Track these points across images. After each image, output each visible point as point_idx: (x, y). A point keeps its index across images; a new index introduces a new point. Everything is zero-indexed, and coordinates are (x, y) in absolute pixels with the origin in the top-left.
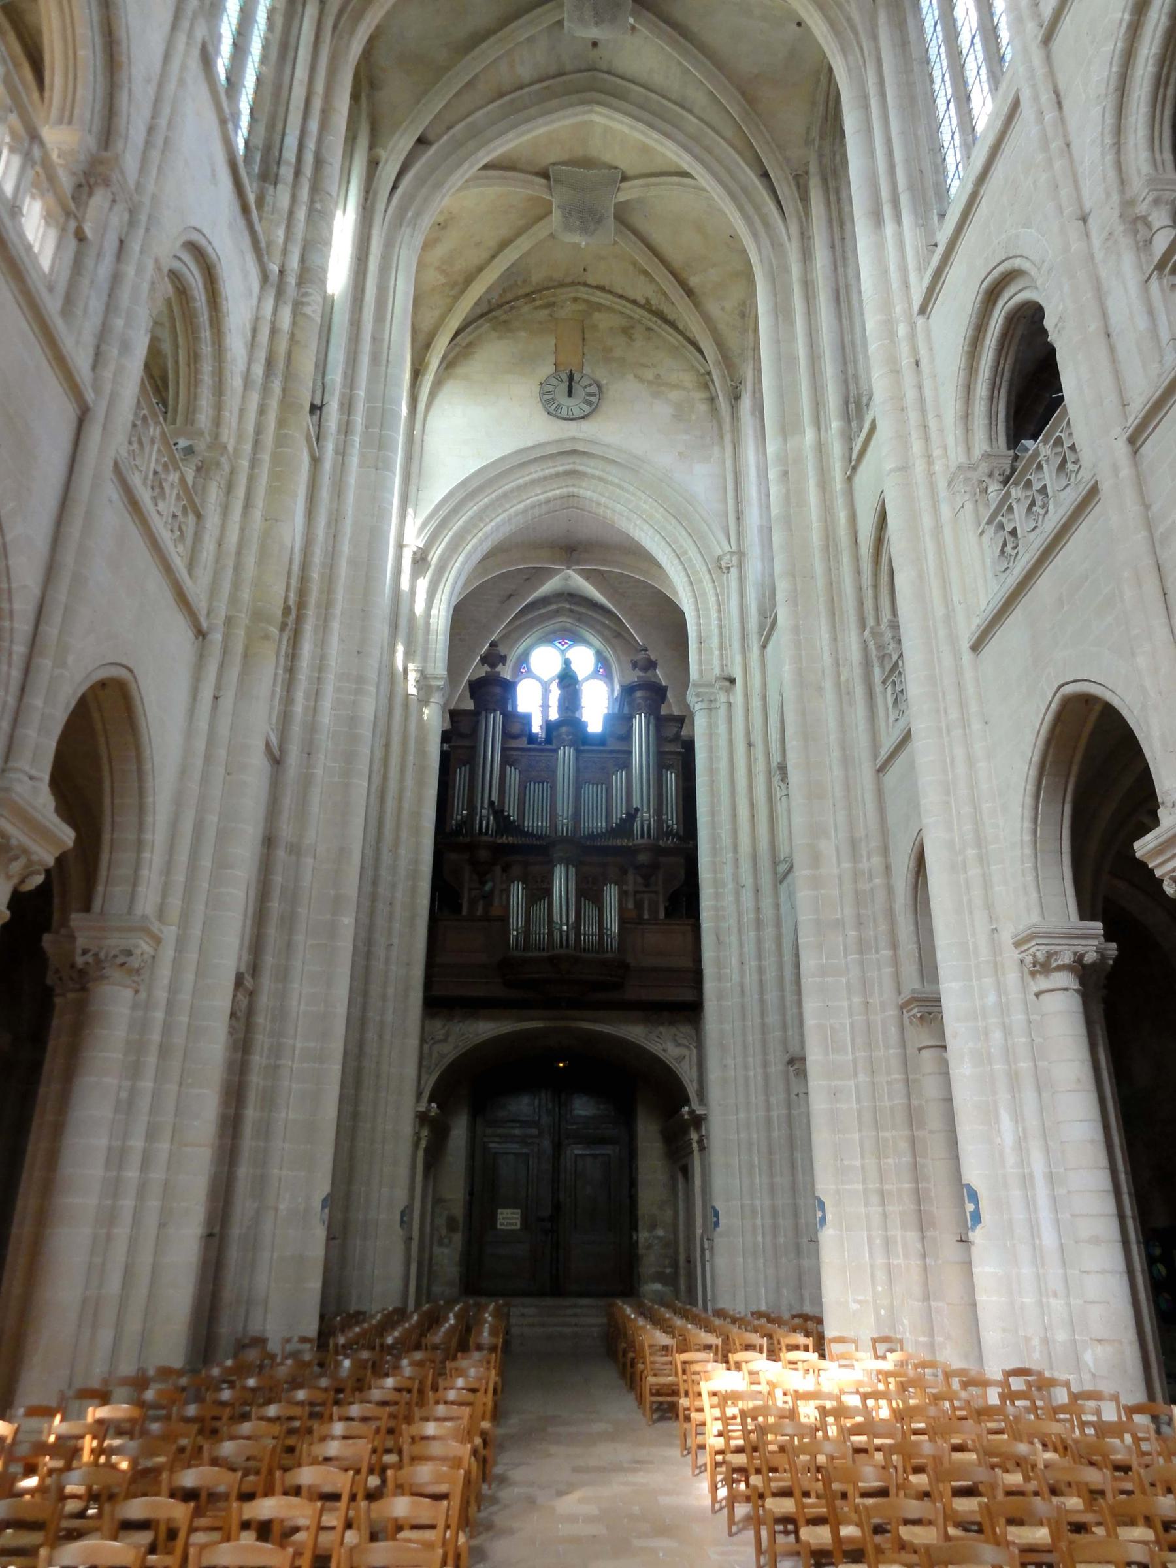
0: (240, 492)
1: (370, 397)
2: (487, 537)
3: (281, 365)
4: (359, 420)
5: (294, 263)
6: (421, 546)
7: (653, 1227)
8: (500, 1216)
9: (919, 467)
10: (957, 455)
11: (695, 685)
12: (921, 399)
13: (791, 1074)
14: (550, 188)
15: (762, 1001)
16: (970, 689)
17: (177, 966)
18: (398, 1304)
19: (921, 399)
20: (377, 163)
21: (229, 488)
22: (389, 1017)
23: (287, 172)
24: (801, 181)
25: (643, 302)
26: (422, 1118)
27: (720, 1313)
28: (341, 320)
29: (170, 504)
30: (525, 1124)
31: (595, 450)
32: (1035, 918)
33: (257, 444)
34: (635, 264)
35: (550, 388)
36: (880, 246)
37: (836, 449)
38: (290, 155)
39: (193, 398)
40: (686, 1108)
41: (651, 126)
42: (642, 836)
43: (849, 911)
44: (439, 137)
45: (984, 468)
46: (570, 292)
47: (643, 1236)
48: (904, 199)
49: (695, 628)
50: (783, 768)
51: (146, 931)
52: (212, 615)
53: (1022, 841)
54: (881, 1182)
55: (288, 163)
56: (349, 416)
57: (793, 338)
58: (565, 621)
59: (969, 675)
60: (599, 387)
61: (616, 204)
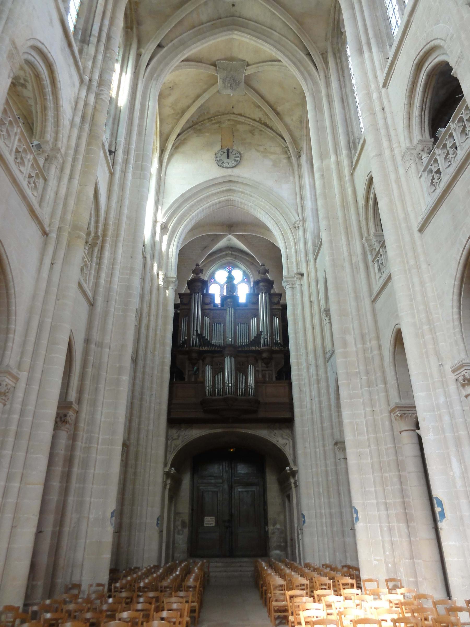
0: (67, 171)
1: (137, 149)
2: (193, 218)
3: (89, 118)
4: (132, 158)
5: (96, 76)
6: (165, 221)
7: (275, 524)
8: (205, 520)
9: (387, 153)
10: (405, 143)
11: (285, 277)
12: (386, 124)
13: (336, 450)
14: (217, 70)
15: (321, 416)
16: (420, 250)
17: (27, 392)
18: (156, 564)
19: (386, 124)
20: (141, 55)
21: (62, 170)
22: (151, 428)
23: (94, 40)
24: (324, 56)
25: (258, 119)
26: (167, 474)
27: (307, 566)
28: (124, 117)
29: (27, 169)
30: (216, 478)
31: (240, 180)
32: (463, 356)
33: (76, 152)
34: (254, 103)
35: (219, 155)
36: (362, 63)
37: (345, 162)
39: (44, 127)
40: (288, 468)
41: (258, 38)
42: (265, 345)
43: (362, 368)
44: (168, 44)
45: (420, 147)
46: (228, 117)
47: (270, 528)
48: (373, 41)
49: (285, 253)
50: (327, 312)
51: (10, 374)
52: (51, 225)
53: (453, 319)
54: (385, 499)
55: (94, 36)
56: (127, 156)
57: (323, 119)
58: (230, 259)
59: (418, 242)
60: (240, 154)
61: (245, 76)
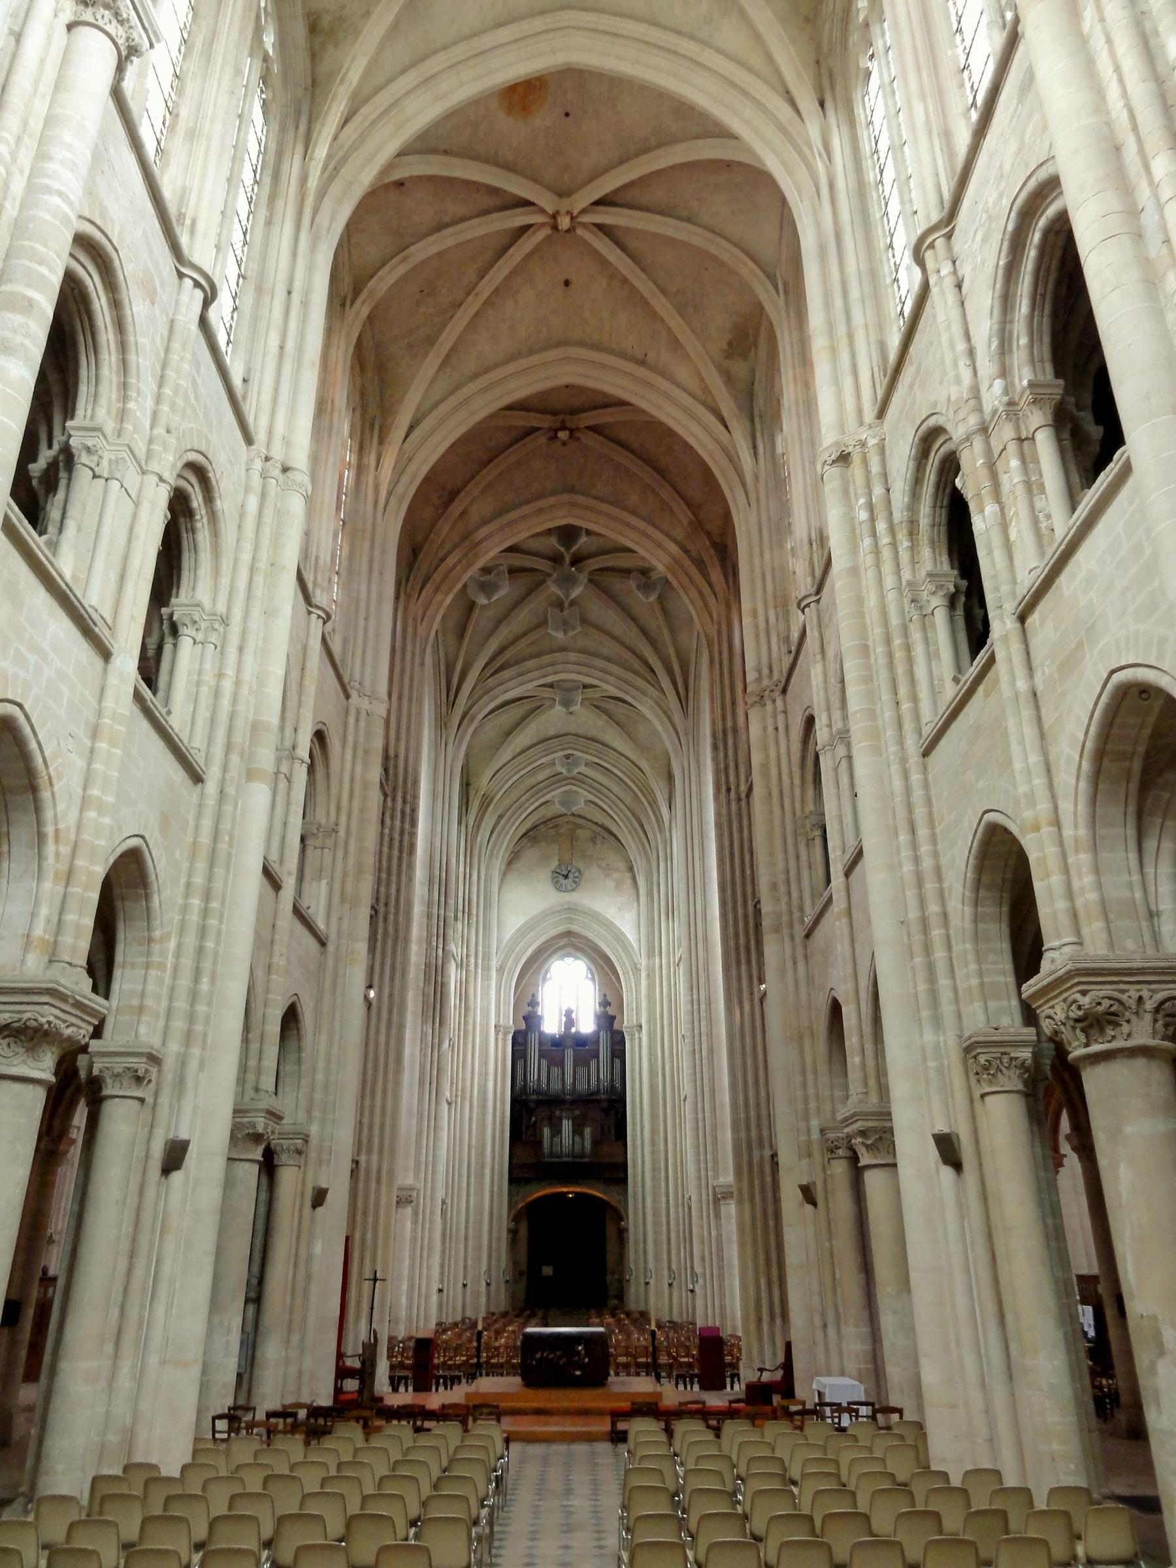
4: (480, 961)
7: (613, 1274)
23: (460, 915)
26: (509, 1231)
38: (460, 907)
46: (565, 819)
47: (609, 1278)
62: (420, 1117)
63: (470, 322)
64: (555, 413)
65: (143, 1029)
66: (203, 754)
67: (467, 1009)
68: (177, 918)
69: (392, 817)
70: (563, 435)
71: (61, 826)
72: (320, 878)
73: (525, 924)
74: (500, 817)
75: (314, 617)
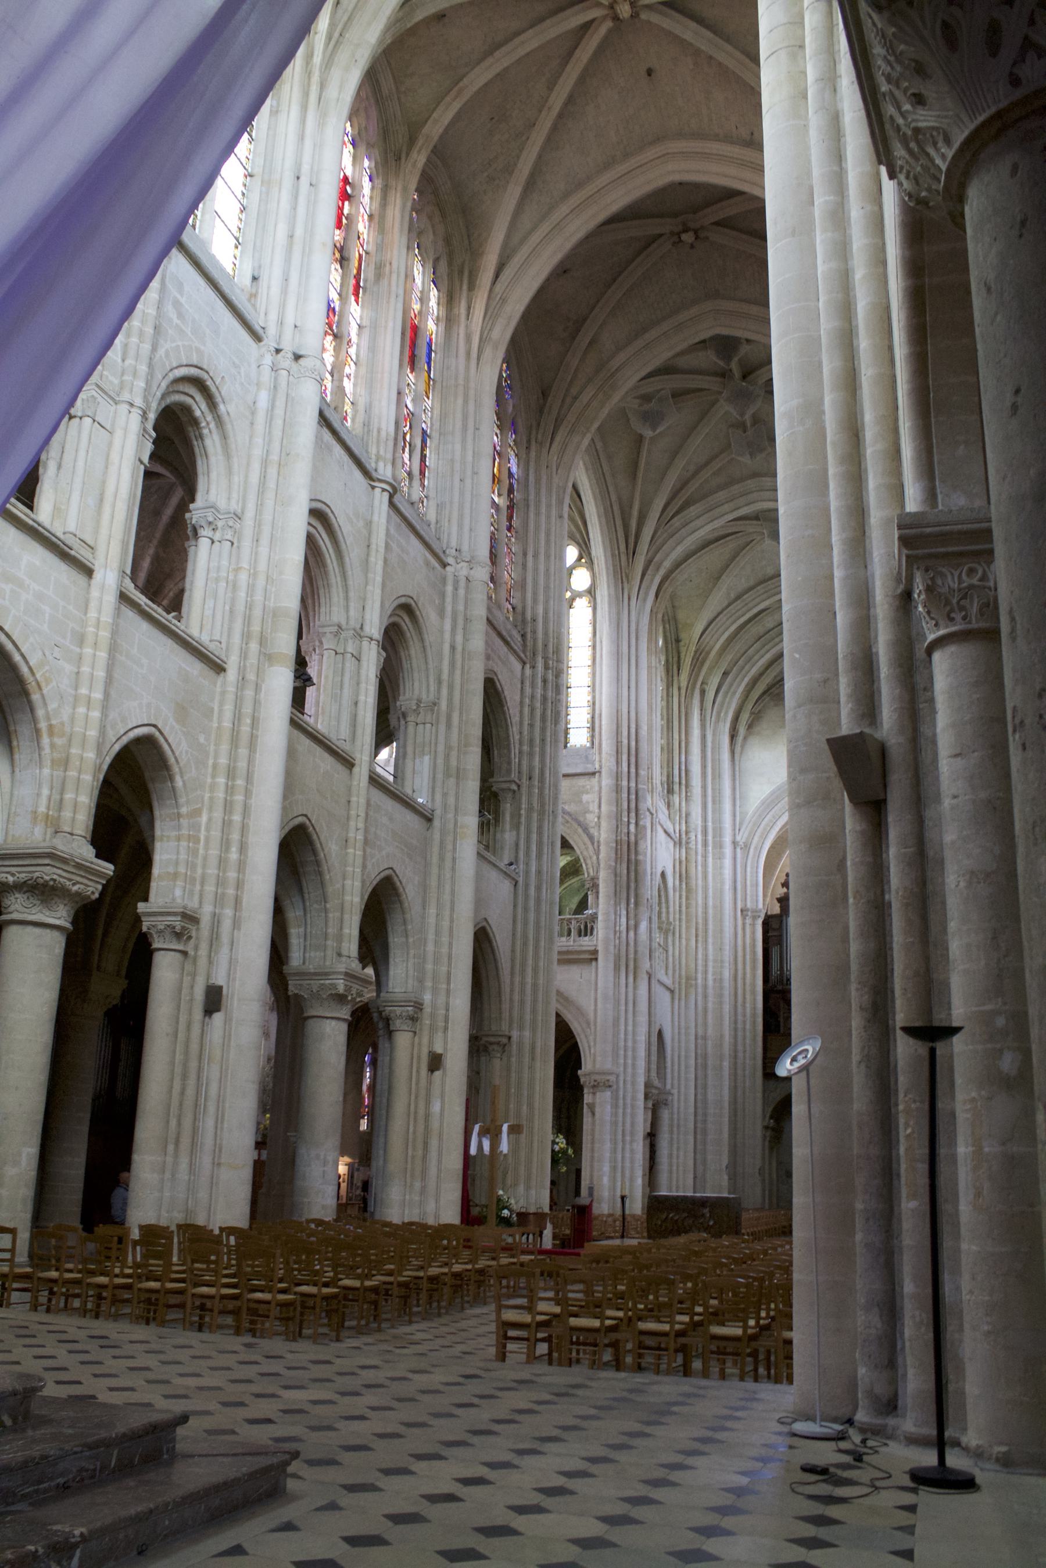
4: (710, 838)
21: (674, 934)
23: (676, 787)
33: (680, 911)
38: (676, 779)
62: (617, 1002)
63: (548, 140)
64: (675, 215)
65: (178, 892)
66: (224, 645)
67: (689, 890)
68: (207, 795)
69: (533, 685)
70: (688, 238)
71: (54, 722)
72: (423, 754)
73: (773, 793)
74: (726, 674)
75: (378, 491)
